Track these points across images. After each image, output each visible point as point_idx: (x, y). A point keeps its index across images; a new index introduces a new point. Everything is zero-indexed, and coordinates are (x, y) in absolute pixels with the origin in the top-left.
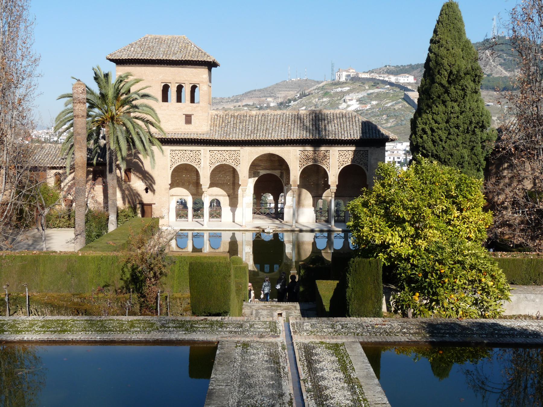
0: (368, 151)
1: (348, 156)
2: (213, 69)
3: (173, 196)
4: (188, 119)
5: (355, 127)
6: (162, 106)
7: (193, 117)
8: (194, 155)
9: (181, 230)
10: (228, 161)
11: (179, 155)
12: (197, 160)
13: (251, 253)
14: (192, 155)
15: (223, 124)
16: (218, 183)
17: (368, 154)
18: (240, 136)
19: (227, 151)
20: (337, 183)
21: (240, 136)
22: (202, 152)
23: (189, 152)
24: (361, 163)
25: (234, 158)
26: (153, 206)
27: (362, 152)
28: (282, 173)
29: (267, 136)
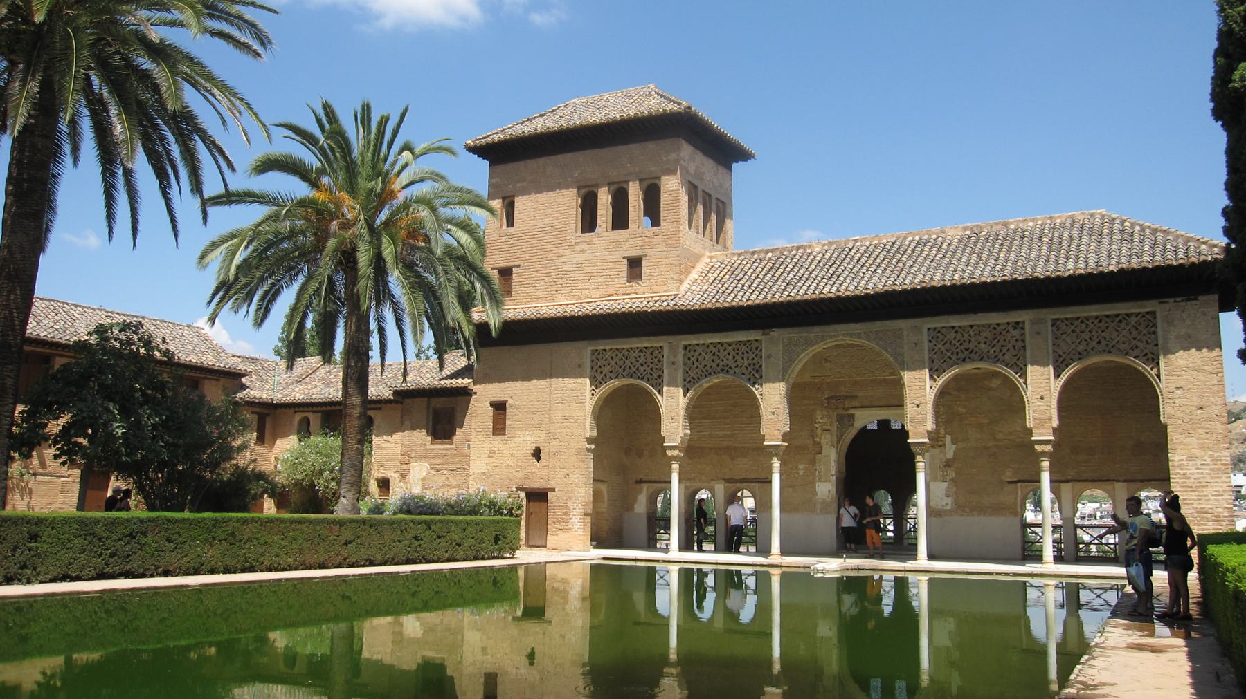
0: (1153, 313)
1: (1086, 336)
2: (736, 167)
3: (641, 482)
5: (1105, 245)
6: (577, 244)
7: (644, 263)
9: (605, 559)
12: (655, 376)
13: (835, 641)
17: (1155, 325)
20: (1055, 423)
22: (666, 352)
23: (637, 354)
24: (1136, 352)
25: (746, 362)
26: (550, 495)
27: (1133, 320)
29: (827, 289)
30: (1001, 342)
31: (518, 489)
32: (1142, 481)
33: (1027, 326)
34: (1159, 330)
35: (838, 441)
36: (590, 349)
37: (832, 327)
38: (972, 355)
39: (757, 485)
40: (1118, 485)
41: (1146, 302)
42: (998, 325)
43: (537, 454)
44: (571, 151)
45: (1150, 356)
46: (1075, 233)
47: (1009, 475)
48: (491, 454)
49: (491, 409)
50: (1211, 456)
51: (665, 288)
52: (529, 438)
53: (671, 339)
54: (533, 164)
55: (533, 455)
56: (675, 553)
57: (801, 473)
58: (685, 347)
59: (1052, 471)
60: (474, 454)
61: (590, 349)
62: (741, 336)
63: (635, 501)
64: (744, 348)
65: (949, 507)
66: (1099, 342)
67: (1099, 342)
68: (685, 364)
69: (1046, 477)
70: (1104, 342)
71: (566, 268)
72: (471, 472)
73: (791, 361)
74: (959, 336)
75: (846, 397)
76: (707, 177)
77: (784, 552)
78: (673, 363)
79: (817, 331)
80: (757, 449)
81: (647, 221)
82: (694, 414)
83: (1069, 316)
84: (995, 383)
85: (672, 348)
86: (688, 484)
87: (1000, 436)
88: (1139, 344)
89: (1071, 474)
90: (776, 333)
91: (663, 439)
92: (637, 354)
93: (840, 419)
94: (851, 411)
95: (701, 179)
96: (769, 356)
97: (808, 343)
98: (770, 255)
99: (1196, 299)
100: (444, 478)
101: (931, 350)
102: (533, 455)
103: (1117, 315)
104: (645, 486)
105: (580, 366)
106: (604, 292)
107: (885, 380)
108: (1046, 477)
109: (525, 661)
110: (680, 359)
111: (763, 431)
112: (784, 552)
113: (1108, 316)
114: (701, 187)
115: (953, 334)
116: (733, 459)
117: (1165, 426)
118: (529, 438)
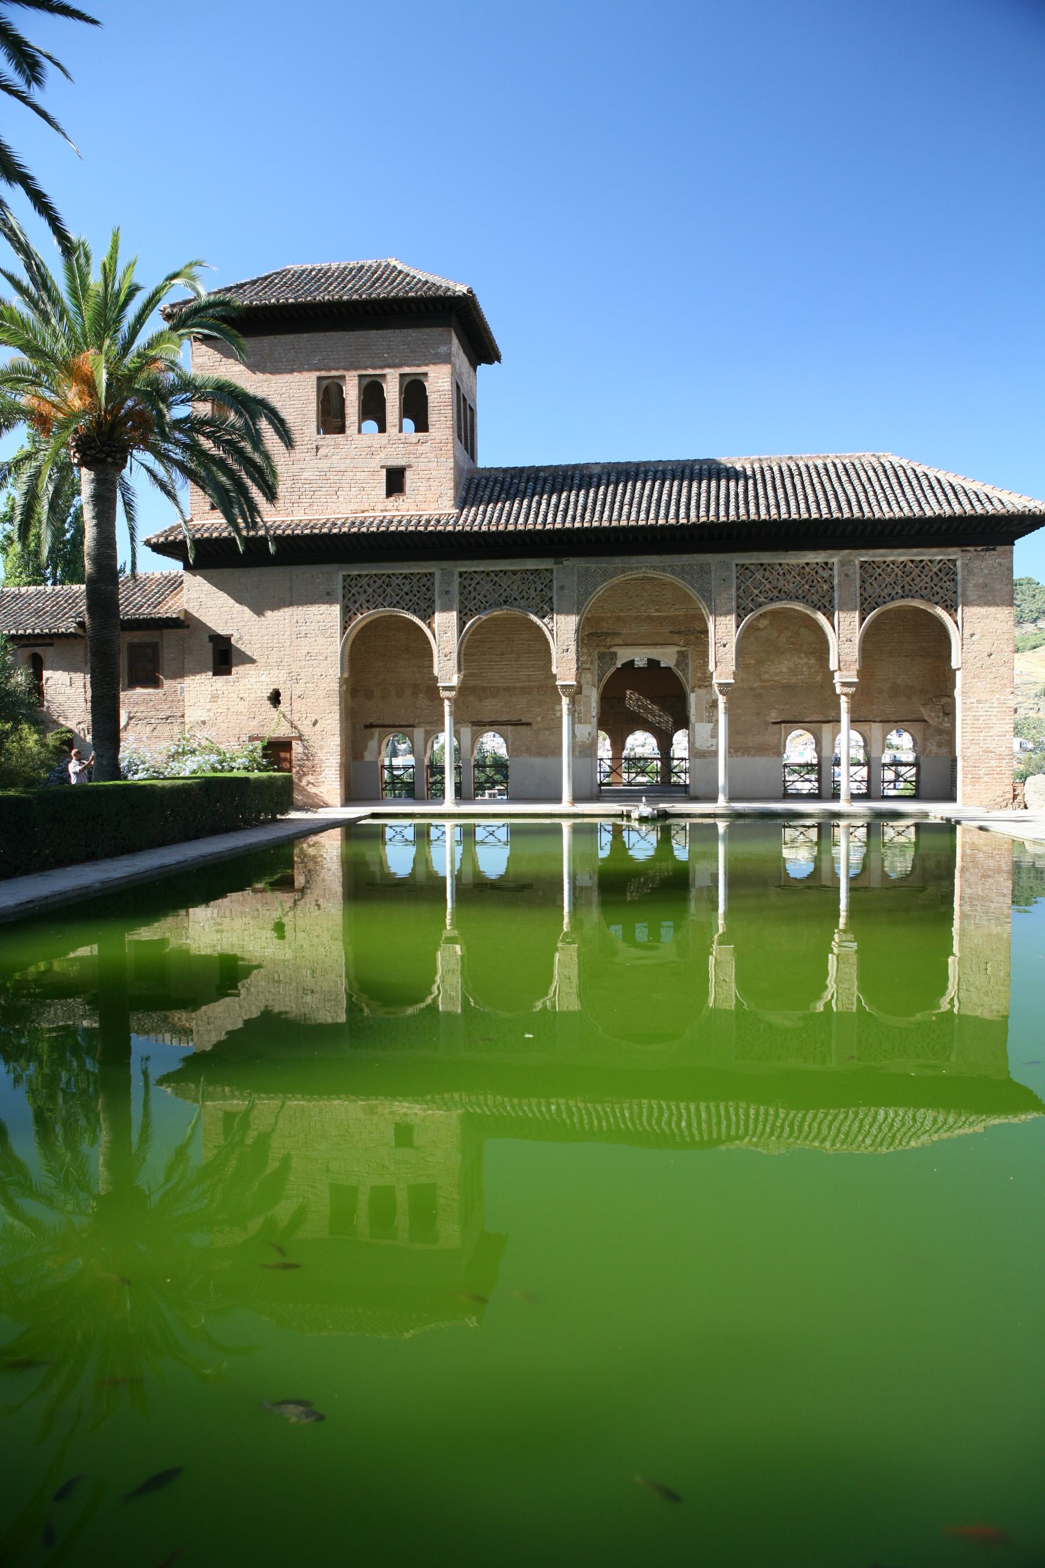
0: (954, 562)
2: (482, 368)
3: (371, 726)
4: (395, 481)
7: (408, 474)
8: (415, 589)
9: (374, 816)
10: (516, 603)
11: (371, 590)
14: (406, 589)
15: (503, 496)
16: (498, 689)
18: (550, 519)
19: (514, 573)
21: (550, 519)
24: (937, 598)
28: (682, 656)
30: (809, 582)
31: (252, 739)
32: (896, 722)
33: (836, 567)
34: (959, 577)
35: (600, 680)
36: (341, 574)
37: (634, 559)
38: (782, 595)
39: (510, 728)
40: (874, 725)
41: (950, 550)
42: (807, 564)
43: (275, 698)
44: (308, 331)
45: (949, 603)
46: (871, 473)
47: (774, 716)
48: (214, 698)
49: (211, 645)
50: (998, 699)
51: (434, 506)
52: (263, 678)
53: (445, 564)
54: (305, 339)
55: (269, 698)
56: (449, 804)
57: (558, 714)
58: (461, 575)
59: (852, 711)
60: (189, 698)
61: (341, 574)
62: (531, 564)
63: (365, 747)
64: (531, 577)
65: (713, 749)
66: (903, 587)
67: (903, 587)
68: (461, 594)
69: (845, 717)
70: (907, 587)
71: (305, 475)
72: (187, 719)
73: (587, 594)
74: (767, 574)
75: (608, 634)
76: (465, 376)
77: (577, 799)
78: (447, 592)
79: (618, 561)
80: (508, 689)
81: (409, 424)
82: (469, 653)
83: (877, 559)
84: (764, 623)
85: (445, 574)
86: (429, 728)
87: (766, 677)
88: (939, 590)
89: (832, 715)
90: (570, 563)
91: (436, 679)
92: (400, 581)
93: (602, 657)
94: (614, 649)
95: (462, 380)
96: (562, 588)
97: (606, 575)
98: (542, 474)
99: (994, 549)
100: (149, 728)
101: (738, 588)
102: (269, 698)
103: (921, 561)
104: (377, 732)
105: (328, 594)
106: (355, 506)
107: (651, 618)
108: (845, 717)
109: (270, 934)
110: (455, 588)
111: (554, 670)
112: (577, 799)
113: (912, 561)
114: (462, 391)
115: (761, 572)
116: (481, 700)
117: (954, 672)
118: (263, 678)
